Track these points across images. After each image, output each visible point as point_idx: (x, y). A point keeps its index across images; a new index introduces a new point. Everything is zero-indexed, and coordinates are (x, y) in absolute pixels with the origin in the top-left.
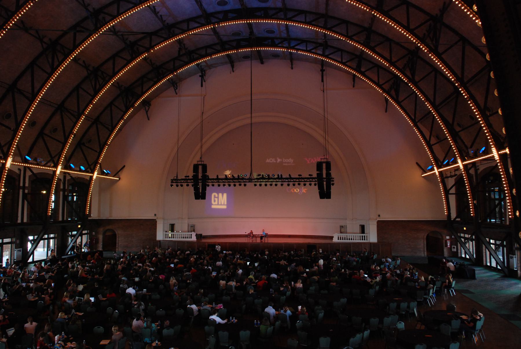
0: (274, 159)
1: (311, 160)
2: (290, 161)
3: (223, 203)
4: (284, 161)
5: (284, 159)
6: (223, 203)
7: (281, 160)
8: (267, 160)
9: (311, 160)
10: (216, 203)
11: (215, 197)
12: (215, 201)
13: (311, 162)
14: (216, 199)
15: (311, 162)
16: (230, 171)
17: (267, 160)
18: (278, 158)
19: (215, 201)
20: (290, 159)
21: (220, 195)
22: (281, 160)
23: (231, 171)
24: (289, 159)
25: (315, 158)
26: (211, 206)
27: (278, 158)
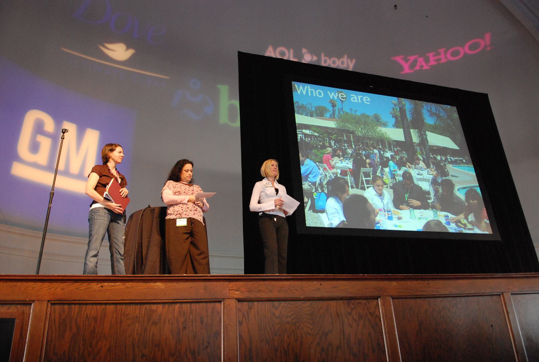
0: (291, 51)
1: (415, 61)
2: (343, 63)
3: (75, 169)
4: (325, 61)
5: (323, 58)
6: (75, 169)
7: (315, 58)
8: (270, 49)
9: (415, 61)
10: (42, 157)
11: (39, 129)
12: (35, 148)
13: (417, 68)
14: (45, 143)
15: (417, 68)
16: (128, 47)
17: (270, 49)
18: (304, 51)
19: (35, 148)
20: (345, 59)
21: (71, 127)
22: (315, 58)
23: (131, 52)
24: (339, 57)
25: (430, 55)
26: (8, 167)
27: (304, 51)
